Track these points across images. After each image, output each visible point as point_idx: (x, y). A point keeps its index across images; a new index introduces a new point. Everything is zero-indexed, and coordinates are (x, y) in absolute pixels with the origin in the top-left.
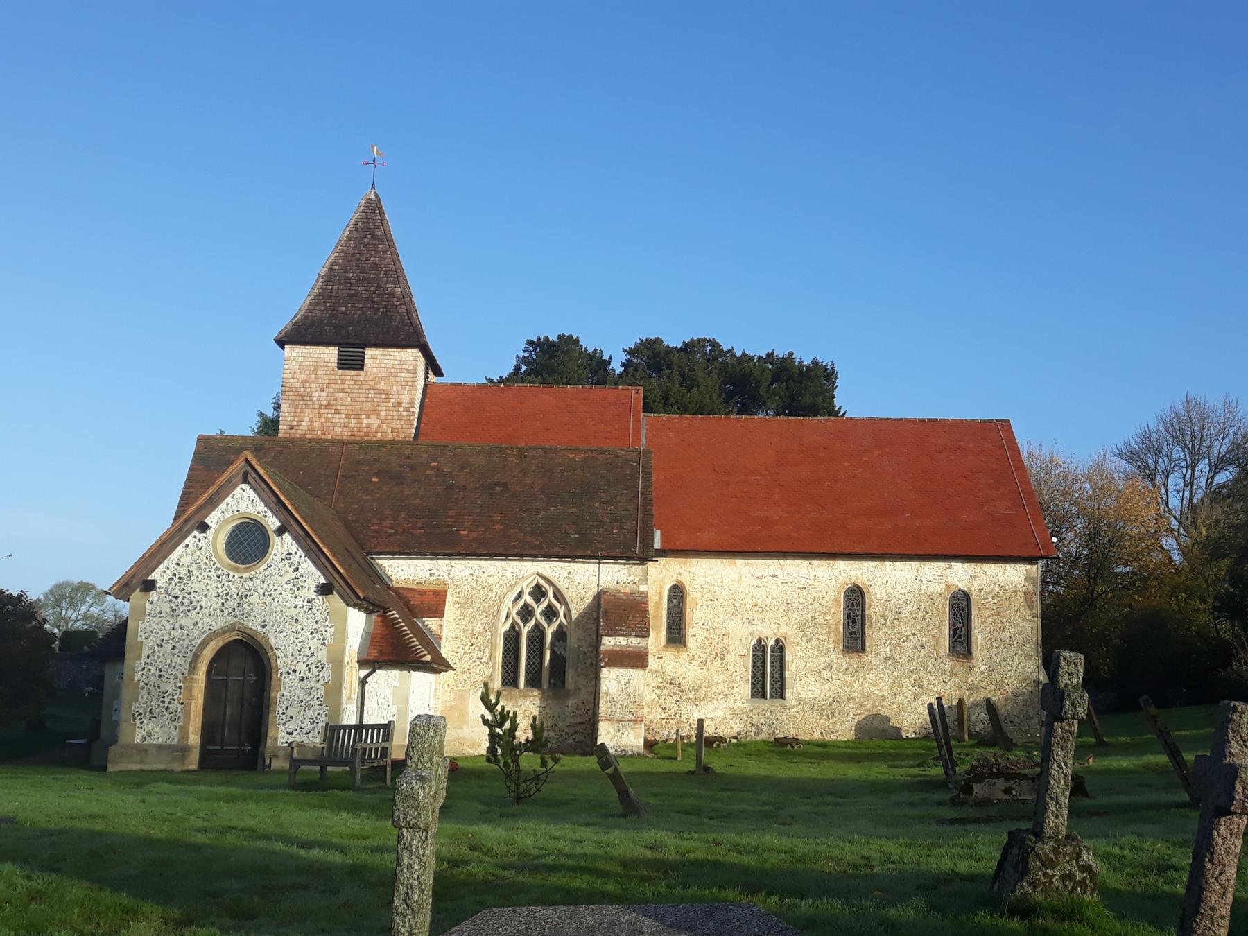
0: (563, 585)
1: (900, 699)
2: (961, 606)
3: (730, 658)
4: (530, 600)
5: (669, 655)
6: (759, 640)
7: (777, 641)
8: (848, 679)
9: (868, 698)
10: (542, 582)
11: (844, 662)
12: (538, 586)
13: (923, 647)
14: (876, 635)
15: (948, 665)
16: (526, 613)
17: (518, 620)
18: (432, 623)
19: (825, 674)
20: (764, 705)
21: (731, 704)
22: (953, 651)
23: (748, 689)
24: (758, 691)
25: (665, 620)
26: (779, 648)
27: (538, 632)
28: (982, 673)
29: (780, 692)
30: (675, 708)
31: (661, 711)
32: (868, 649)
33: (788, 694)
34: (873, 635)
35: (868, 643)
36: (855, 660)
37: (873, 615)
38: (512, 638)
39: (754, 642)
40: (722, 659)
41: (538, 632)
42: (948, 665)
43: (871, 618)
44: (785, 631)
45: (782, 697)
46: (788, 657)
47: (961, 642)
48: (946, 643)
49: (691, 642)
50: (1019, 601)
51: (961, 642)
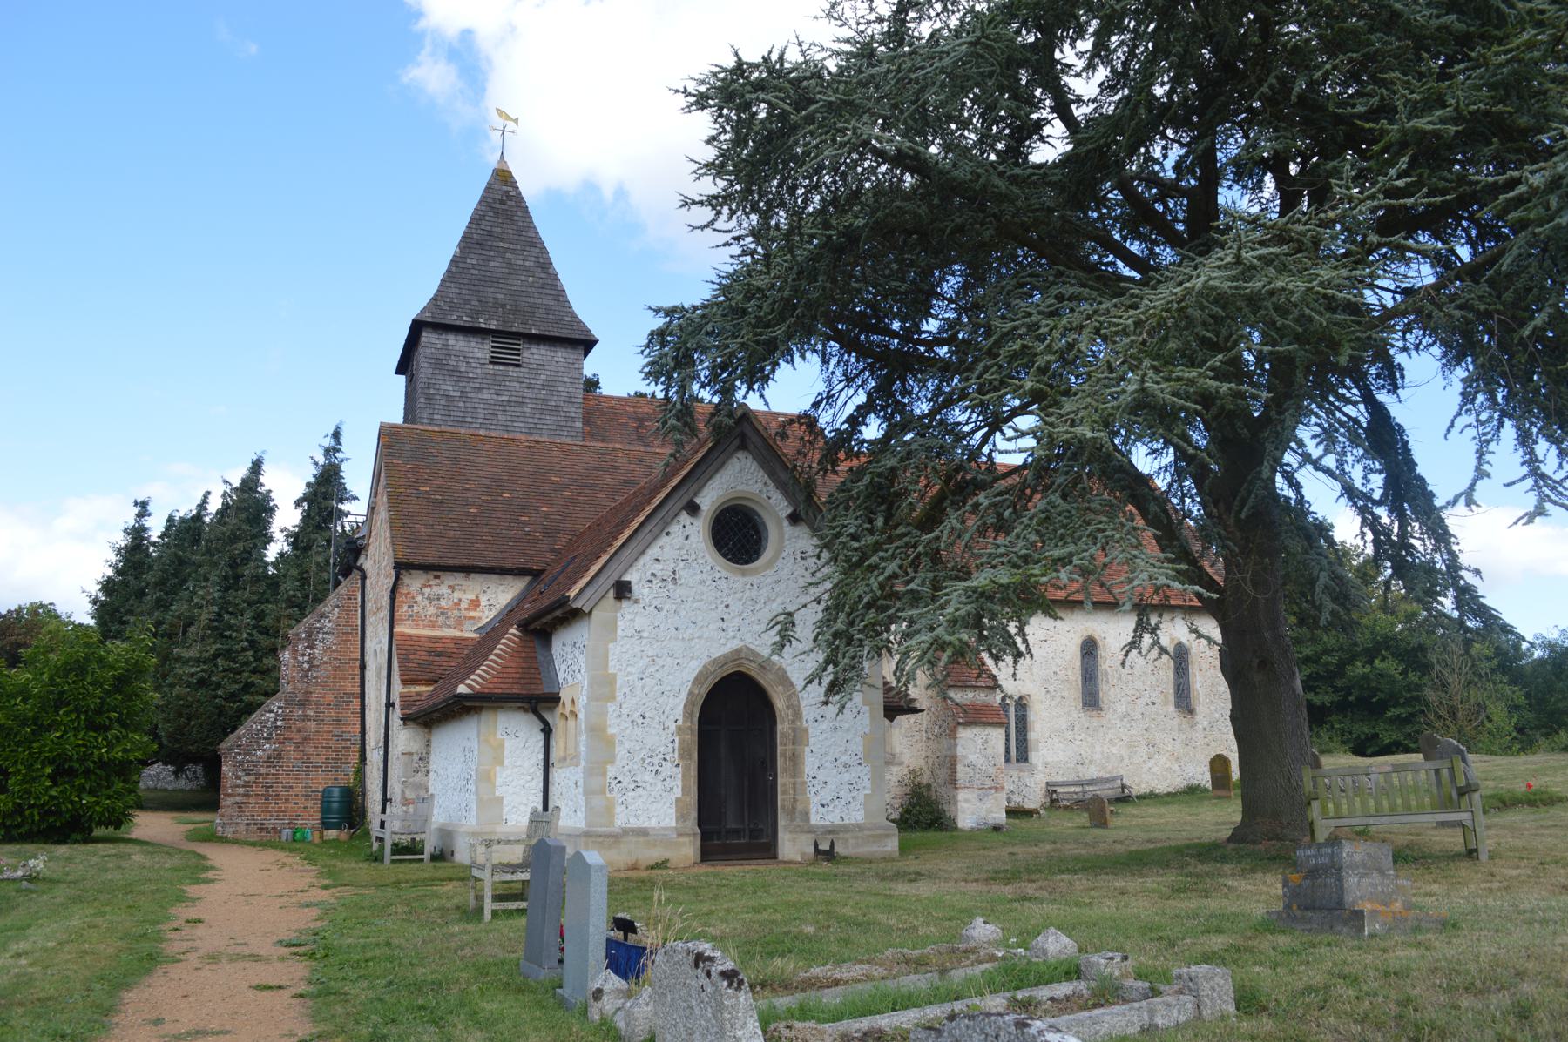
9: (1108, 759)
11: (1085, 721)
15: (1176, 721)
19: (1069, 735)
22: (1177, 706)
29: (1023, 757)
32: (1105, 707)
33: (1034, 757)
34: (1109, 691)
45: (1026, 760)
46: (1032, 716)
48: (1172, 699)
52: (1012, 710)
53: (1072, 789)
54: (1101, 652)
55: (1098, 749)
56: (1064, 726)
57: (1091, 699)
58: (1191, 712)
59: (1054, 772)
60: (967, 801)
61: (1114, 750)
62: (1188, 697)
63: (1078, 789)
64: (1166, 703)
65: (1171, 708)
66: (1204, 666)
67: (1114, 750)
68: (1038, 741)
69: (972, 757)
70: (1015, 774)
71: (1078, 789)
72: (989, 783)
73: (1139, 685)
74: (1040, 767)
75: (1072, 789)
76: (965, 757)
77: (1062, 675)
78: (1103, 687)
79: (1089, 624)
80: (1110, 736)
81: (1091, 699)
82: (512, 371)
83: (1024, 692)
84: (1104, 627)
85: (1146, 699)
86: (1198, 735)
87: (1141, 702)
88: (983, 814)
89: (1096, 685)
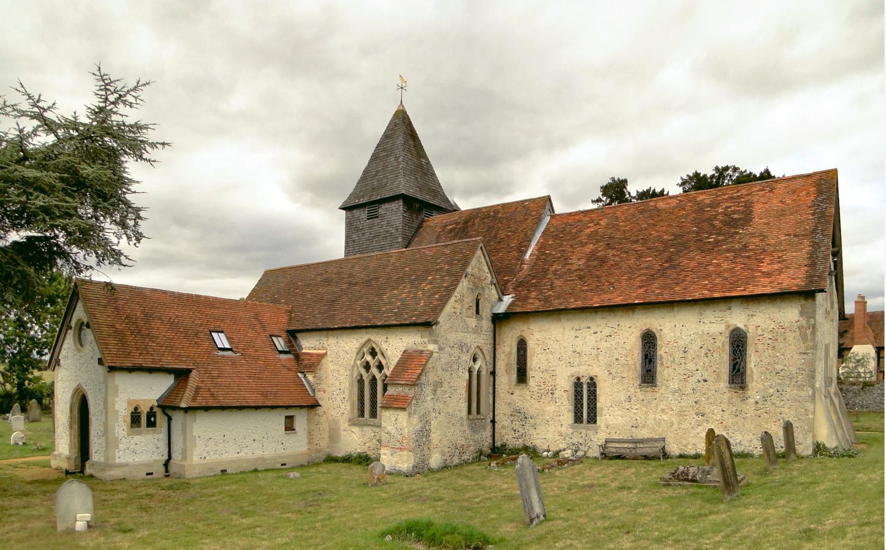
0: (384, 346)
1: (686, 425)
2: (738, 343)
4: (368, 358)
5: (517, 392)
6: (578, 379)
7: (592, 379)
8: (644, 409)
9: (659, 424)
10: (374, 346)
12: (373, 349)
13: (705, 381)
14: (666, 372)
15: (727, 396)
16: (367, 367)
17: (363, 371)
18: (310, 377)
19: (627, 405)
20: (583, 428)
21: (559, 428)
22: (732, 381)
24: (578, 419)
25: (515, 367)
26: (592, 384)
27: (374, 381)
28: (757, 403)
29: (592, 419)
30: (521, 429)
31: (513, 432)
34: (662, 372)
35: (659, 377)
36: (648, 394)
37: (664, 355)
38: (361, 381)
39: (573, 380)
40: (552, 394)
41: (374, 381)
42: (727, 396)
43: (661, 358)
44: (595, 371)
45: (595, 422)
47: (738, 374)
48: (725, 376)
49: (532, 382)
50: (790, 336)
51: (738, 374)
52: (585, 387)
53: (626, 445)
54: (659, 342)
55: (651, 416)
59: (613, 431)
60: (385, 454)
61: (665, 417)
62: (743, 374)
63: (630, 445)
64: (718, 379)
65: (724, 384)
66: (760, 347)
67: (665, 417)
68: (602, 409)
69: (389, 428)
70: (584, 431)
71: (630, 445)
72: (398, 445)
73: (691, 366)
74: (603, 428)
75: (626, 445)
76: (385, 428)
77: (622, 360)
79: (648, 320)
80: (663, 407)
81: (648, 375)
82: (376, 221)
83: (592, 374)
84: (661, 321)
85: (698, 376)
86: (749, 408)
87: (692, 380)
88: (393, 464)
89: (655, 367)
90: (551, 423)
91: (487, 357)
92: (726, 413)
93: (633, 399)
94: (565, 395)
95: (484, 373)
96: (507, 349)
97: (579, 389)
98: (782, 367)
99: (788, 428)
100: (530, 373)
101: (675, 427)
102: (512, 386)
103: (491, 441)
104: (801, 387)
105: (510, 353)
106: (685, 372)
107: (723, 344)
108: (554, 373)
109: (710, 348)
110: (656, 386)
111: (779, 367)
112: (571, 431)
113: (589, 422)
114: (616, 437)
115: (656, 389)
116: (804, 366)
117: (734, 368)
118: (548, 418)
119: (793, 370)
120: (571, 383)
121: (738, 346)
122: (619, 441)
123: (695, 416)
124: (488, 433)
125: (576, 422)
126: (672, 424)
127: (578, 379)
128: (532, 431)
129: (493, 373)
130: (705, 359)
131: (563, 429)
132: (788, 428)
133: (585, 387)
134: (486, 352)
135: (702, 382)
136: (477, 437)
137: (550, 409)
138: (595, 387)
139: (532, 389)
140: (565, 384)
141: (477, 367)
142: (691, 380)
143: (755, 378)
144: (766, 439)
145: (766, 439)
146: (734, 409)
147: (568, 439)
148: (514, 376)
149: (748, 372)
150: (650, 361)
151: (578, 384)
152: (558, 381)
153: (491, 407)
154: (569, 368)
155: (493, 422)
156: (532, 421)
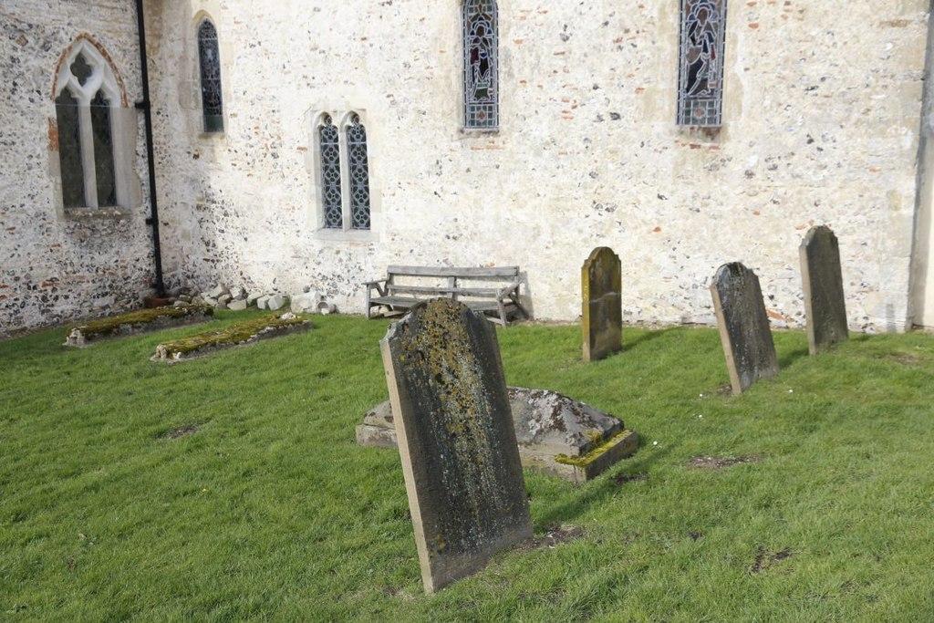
3: (286, 154)
13: (616, 116)
15: (673, 154)
19: (433, 183)
20: (343, 239)
22: (685, 115)
23: (310, 210)
24: (332, 218)
26: (358, 133)
28: (749, 175)
29: (362, 219)
31: (204, 248)
32: (503, 126)
34: (511, 93)
35: (504, 111)
36: (477, 152)
37: (514, 49)
43: (508, 57)
45: (368, 225)
49: (231, 125)
52: (342, 136)
56: (423, 167)
57: (480, 108)
58: (713, 132)
64: (649, 112)
70: (344, 247)
71: (444, 284)
73: (581, 78)
78: (504, 86)
81: (480, 108)
83: (355, 107)
85: (597, 105)
87: (583, 116)
90: (276, 225)
91: (123, 66)
92: (667, 205)
93: (447, 167)
94: (300, 158)
95: (116, 104)
96: (178, 49)
97: (331, 144)
98: (822, 69)
99: (821, 250)
100: (229, 106)
101: (545, 237)
102: (195, 139)
103: (152, 269)
104: (880, 127)
105: (183, 58)
106: (565, 93)
107: (662, 11)
108: (275, 106)
109: (628, 24)
110: (496, 133)
111: (814, 71)
112: (318, 246)
113: (355, 225)
114: (411, 262)
115: (498, 141)
116: (892, 65)
117: (692, 79)
118: (269, 214)
119: (858, 75)
120: (311, 131)
121: (703, 15)
122: (417, 274)
123: (591, 211)
124: (139, 249)
125: (328, 224)
126: (537, 232)
127: (327, 117)
128: (239, 244)
129: (144, 106)
130: (618, 55)
131: (301, 242)
132: (821, 250)
133: (342, 136)
134: (114, 52)
135: (607, 118)
136: (100, 259)
137: (274, 191)
138: (364, 139)
139: (235, 146)
140: (302, 135)
141: (86, 93)
142: (580, 114)
143: (746, 101)
144: (738, 286)
145: (738, 286)
146: (689, 191)
147: (312, 264)
148: (198, 114)
149: (728, 88)
150: (484, 66)
151: (327, 134)
152: (285, 127)
153: (147, 188)
154: (306, 90)
155: (153, 222)
156: (237, 222)
